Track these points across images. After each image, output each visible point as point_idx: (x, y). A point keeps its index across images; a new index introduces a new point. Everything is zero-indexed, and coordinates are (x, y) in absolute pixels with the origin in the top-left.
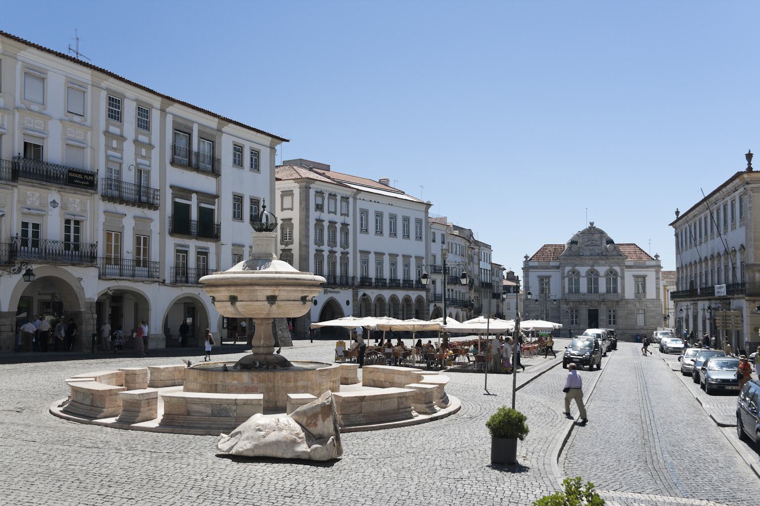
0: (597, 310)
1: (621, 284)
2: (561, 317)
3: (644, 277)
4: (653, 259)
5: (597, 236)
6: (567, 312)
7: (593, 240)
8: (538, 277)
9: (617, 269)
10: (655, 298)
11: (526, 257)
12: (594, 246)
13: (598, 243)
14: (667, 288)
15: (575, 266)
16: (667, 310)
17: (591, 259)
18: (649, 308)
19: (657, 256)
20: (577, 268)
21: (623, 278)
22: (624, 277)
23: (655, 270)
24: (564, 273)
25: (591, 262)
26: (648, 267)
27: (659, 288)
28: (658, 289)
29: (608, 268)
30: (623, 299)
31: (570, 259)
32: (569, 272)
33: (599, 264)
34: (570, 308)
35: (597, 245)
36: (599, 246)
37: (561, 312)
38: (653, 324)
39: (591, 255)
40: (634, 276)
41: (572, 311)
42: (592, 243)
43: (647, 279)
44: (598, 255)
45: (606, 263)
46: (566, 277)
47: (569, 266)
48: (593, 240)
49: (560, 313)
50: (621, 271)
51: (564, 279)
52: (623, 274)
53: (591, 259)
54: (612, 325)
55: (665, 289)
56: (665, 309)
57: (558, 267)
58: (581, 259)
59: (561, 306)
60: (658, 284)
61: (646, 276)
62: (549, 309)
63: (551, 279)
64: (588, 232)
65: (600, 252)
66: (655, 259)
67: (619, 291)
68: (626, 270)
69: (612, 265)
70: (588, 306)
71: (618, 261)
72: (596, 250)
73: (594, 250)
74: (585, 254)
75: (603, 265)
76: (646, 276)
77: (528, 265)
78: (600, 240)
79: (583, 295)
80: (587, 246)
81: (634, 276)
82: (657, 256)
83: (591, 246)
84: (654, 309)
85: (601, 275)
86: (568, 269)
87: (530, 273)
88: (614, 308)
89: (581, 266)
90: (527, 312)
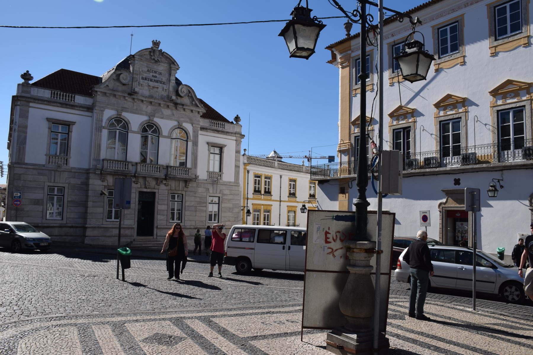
0: (154, 193)
1: (192, 153)
2: (90, 204)
3: (221, 148)
4: (232, 123)
5: (162, 67)
6: (102, 194)
7: (155, 72)
8: (48, 120)
9: (188, 127)
10: (232, 179)
11: (26, 76)
12: (157, 81)
13: (164, 79)
14: (248, 168)
15: (122, 111)
16: (246, 200)
17: (151, 103)
18: (225, 195)
19: (237, 119)
20: (126, 115)
21: (195, 144)
22: (197, 142)
23: (234, 138)
24: (102, 121)
25: (150, 109)
26: (227, 133)
27: (239, 167)
28: (237, 167)
29: (175, 123)
30: (196, 177)
31: (115, 96)
32: (110, 119)
33: (162, 113)
34: (108, 187)
35: (161, 82)
36: (164, 83)
37: (90, 193)
38: (229, 221)
39: (151, 97)
40: (208, 143)
41: (111, 194)
42: (153, 76)
43: (225, 150)
44: (162, 98)
45: (173, 115)
46: (104, 128)
47: (112, 109)
48: (155, 72)
49: (87, 196)
50: (194, 131)
51: (101, 131)
52: (196, 136)
53: (151, 103)
54: (113, 220)
55: (245, 169)
56: (244, 198)
57: (90, 109)
58: (134, 99)
59: (91, 181)
60: (237, 160)
61: (225, 146)
62: (66, 186)
63: (75, 129)
64: (148, 57)
65: (165, 94)
66: (235, 123)
67: (189, 165)
68: (200, 132)
69: (182, 119)
70: (139, 185)
71: (191, 114)
72: (160, 89)
73: (156, 89)
74: (141, 91)
75: (169, 118)
76: (225, 146)
77: (29, 92)
78: (167, 75)
79: (132, 165)
80: (146, 79)
81: (208, 143)
82: (237, 119)
83: (151, 81)
84: (230, 197)
85: (164, 134)
86: (109, 113)
87: (30, 109)
88: (180, 192)
89: (132, 112)
90: (18, 190)
